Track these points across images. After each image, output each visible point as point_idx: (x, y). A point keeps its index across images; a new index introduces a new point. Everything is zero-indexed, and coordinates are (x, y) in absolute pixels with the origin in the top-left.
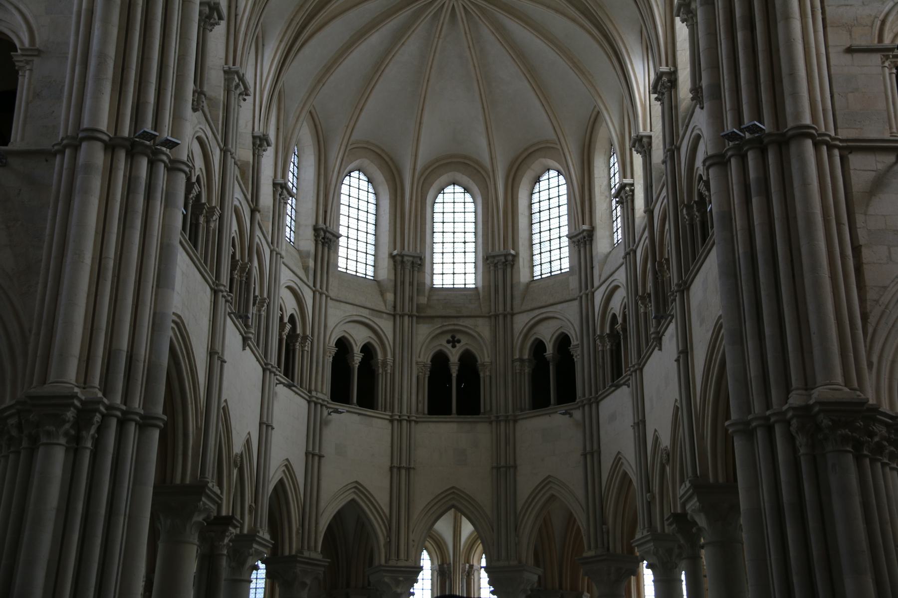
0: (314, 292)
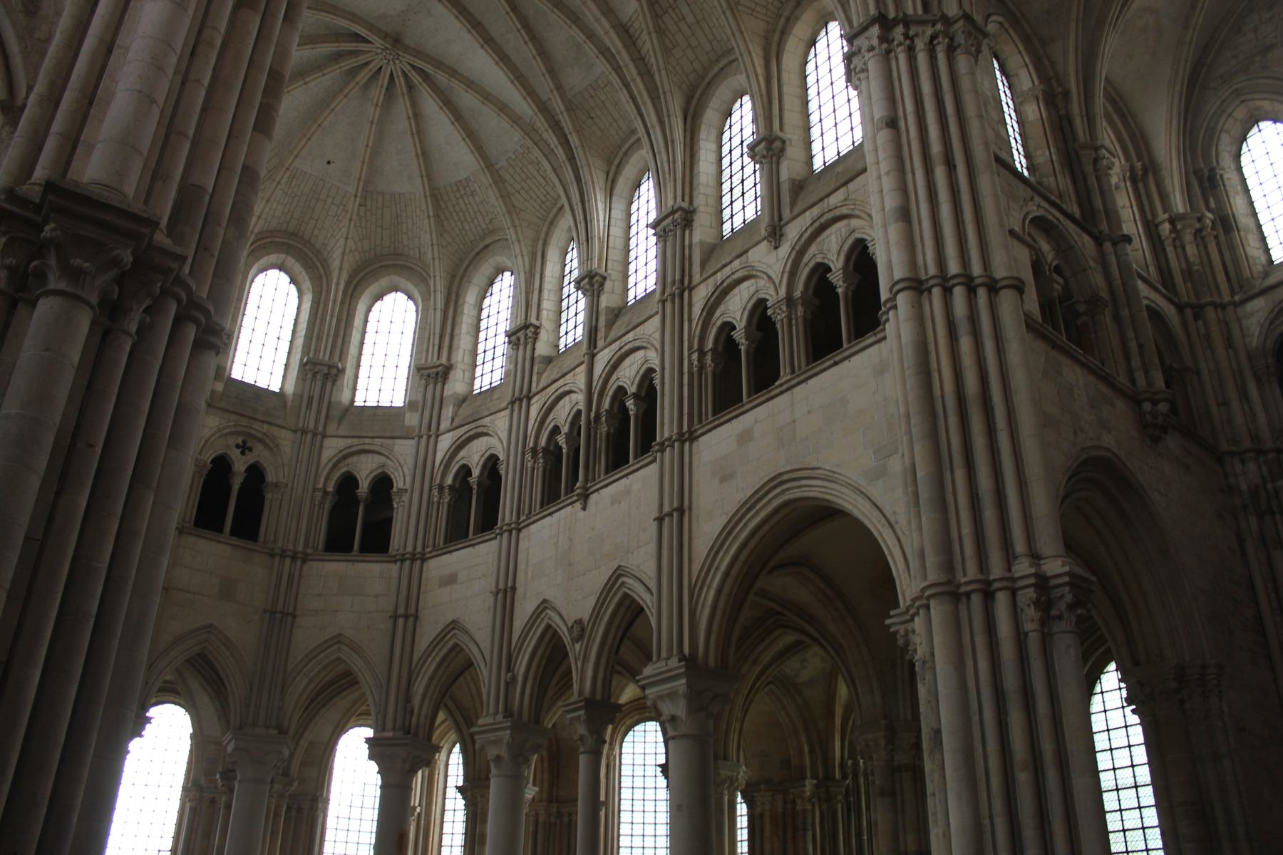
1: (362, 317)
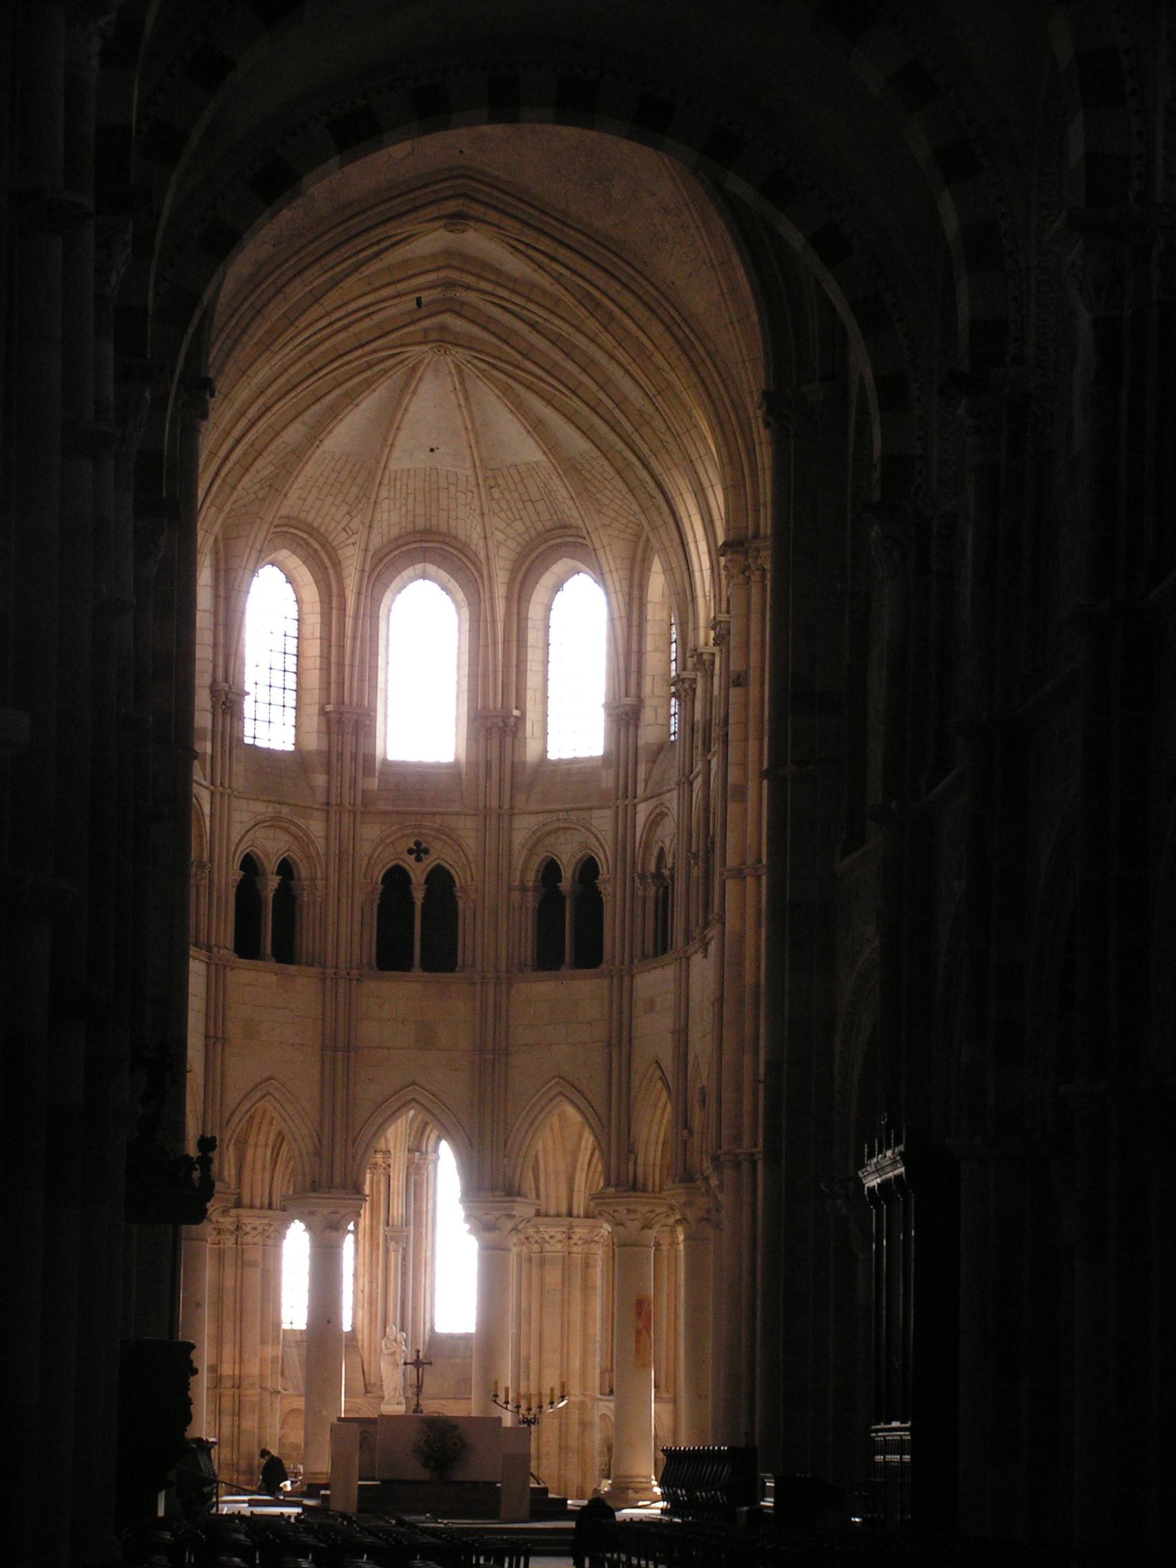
0: (212, 794)
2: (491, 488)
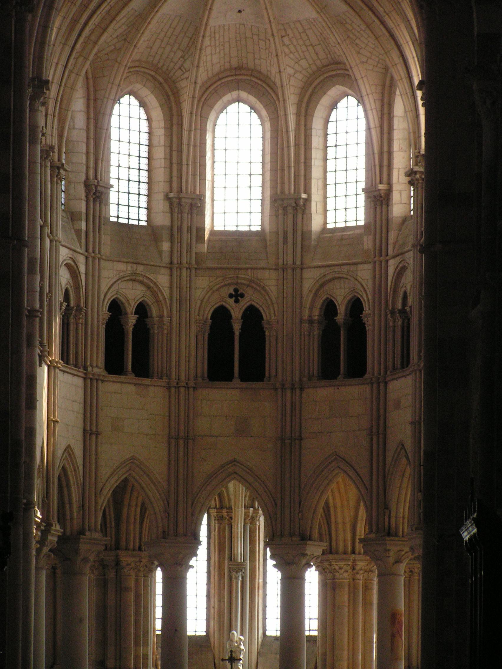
0: (87, 258)
1: (321, 133)
2: (282, 37)
